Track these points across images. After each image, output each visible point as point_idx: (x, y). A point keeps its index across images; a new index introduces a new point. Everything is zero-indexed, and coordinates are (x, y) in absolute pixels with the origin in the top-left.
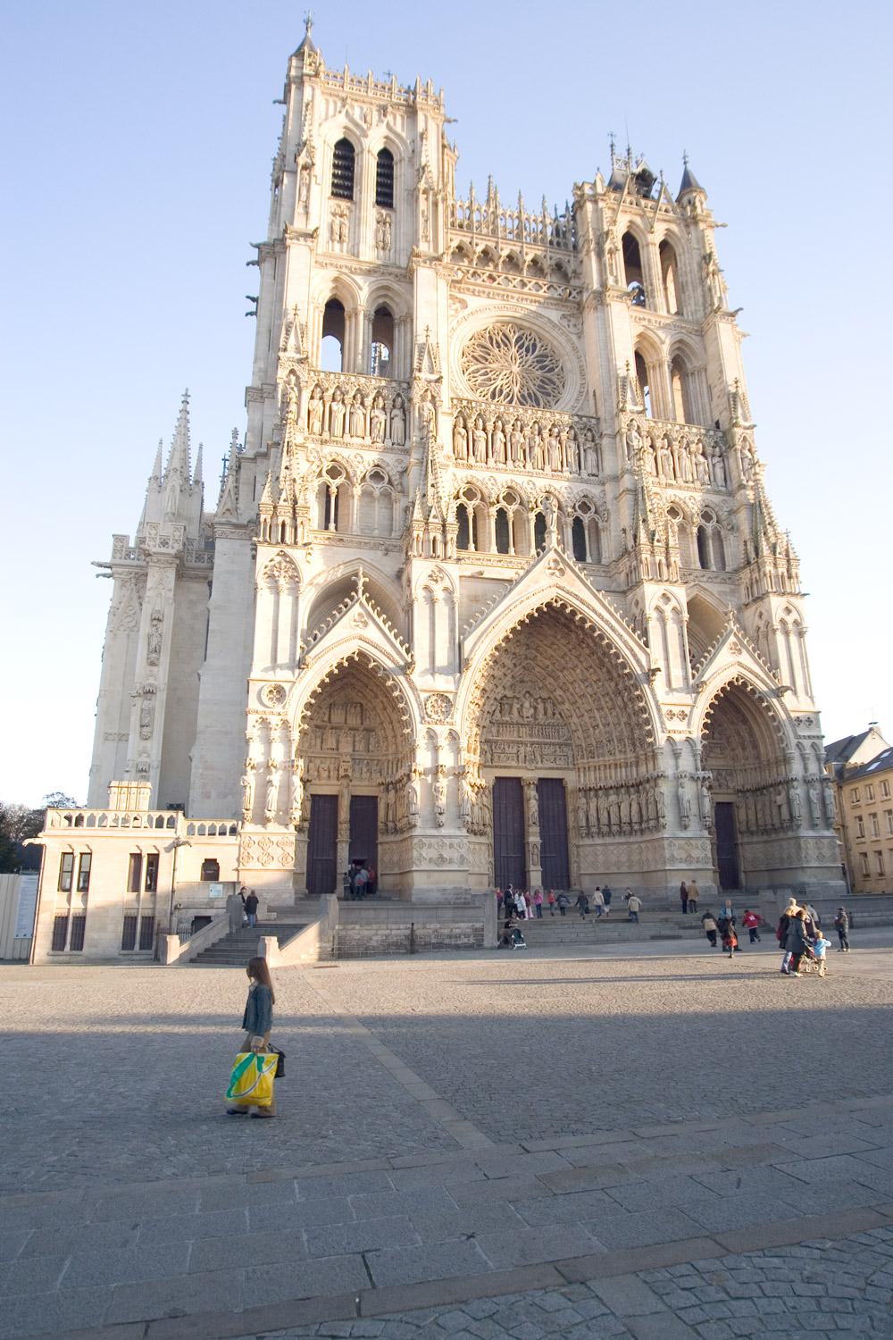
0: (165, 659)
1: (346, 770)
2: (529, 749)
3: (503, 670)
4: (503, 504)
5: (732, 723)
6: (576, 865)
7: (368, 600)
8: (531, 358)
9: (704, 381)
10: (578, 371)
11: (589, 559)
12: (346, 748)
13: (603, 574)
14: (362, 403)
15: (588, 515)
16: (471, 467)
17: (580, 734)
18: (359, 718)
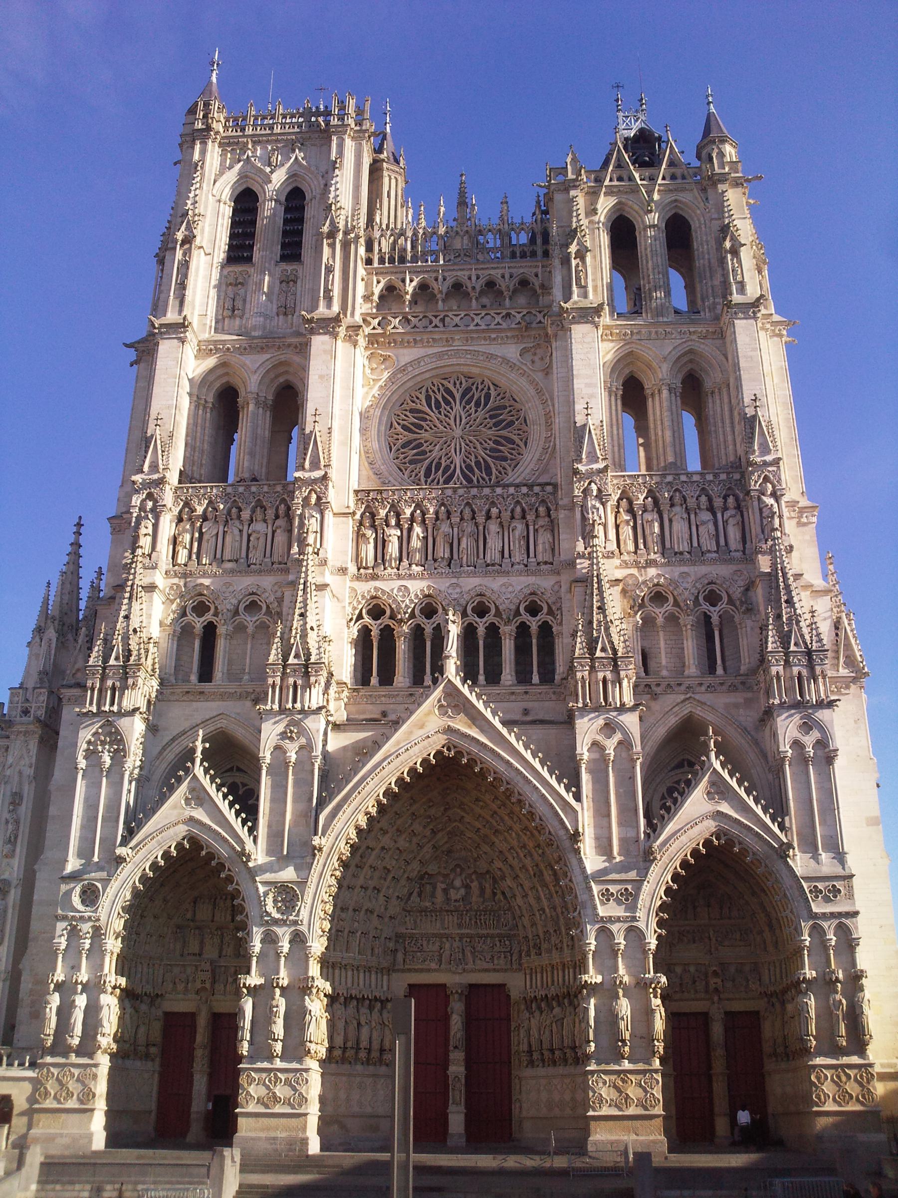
0: (20, 849)
1: (203, 982)
2: (456, 944)
3: (415, 840)
4: (421, 620)
5: (754, 894)
6: (518, 1105)
7: (206, 771)
8: (481, 413)
9: (726, 400)
10: (543, 421)
11: (536, 679)
12: (211, 952)
13: (553, 697)
14: (239, 517)
15: (538, 618)
16: (375, 577)
17: (526, 921)
18: (229, 912)
